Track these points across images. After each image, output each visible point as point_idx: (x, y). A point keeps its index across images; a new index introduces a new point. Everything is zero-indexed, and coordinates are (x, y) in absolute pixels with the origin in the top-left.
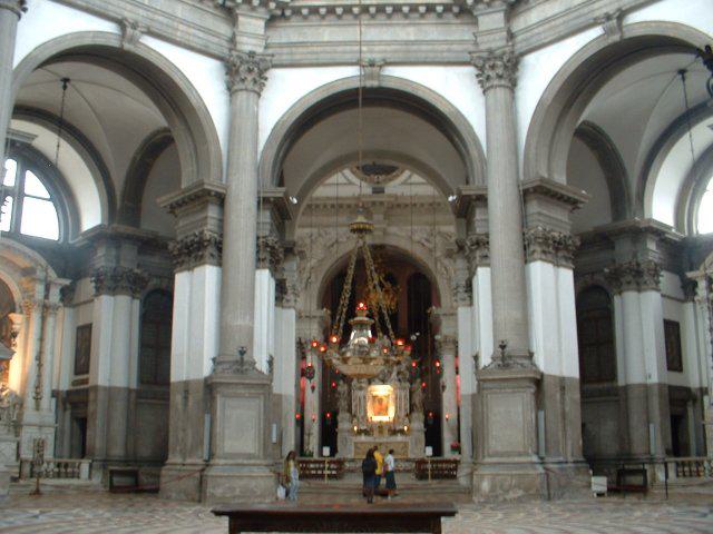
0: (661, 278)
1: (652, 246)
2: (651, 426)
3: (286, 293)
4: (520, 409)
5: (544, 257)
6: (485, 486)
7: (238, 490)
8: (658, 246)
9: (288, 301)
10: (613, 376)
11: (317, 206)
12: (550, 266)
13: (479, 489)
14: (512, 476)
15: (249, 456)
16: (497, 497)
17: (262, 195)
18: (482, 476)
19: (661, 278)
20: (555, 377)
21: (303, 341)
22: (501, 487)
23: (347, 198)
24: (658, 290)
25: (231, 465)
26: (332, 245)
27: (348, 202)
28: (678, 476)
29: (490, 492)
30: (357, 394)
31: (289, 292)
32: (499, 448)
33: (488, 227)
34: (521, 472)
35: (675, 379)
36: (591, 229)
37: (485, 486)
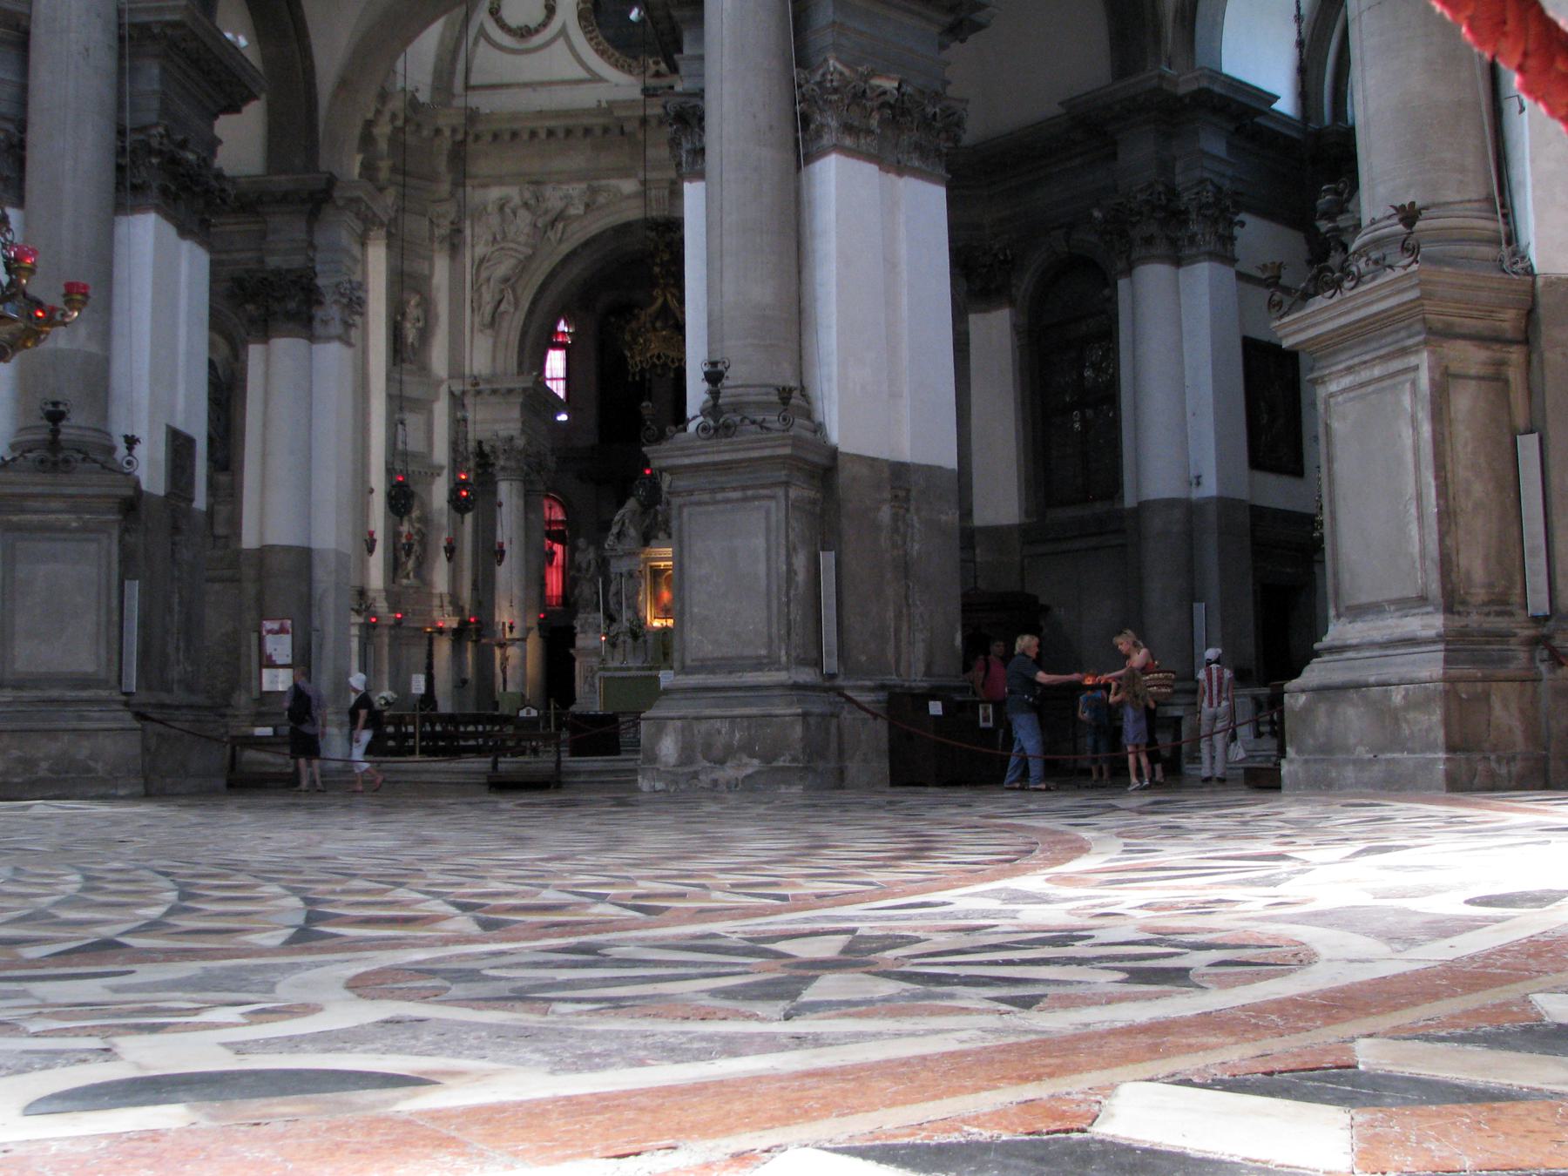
0: (1237, 231)
1: (1215, 145)
2: (1199, 609)
3: (320, 303)
4: (760, 543)
5: (848, 141)
6: (668, 748)
7: (44, 765)
8: (1230, 146)
9: (325, 323)
10: (1114, 487)
11: (514, 135)
12: (871, 169)
13: (652, 758)
14: (733, 717)
15: (84, 682)
16: (695, 775)
17: (126, 19)
18: (661, 723)
19: (1237, 231)
20: (872, 462)
21: (486, 448)
22: (708, 747)
23: (586, 112)
24: (1230, 260)
25: (31, 703)
26: (553, 223)
27: (586, 121)
28: (1259, 735)
29: (681, 764)
30: (618, 566)
31: (329, 299)
32: (709, 650)
33: (702, 76)
34: (754, 711)
35: (1275, 492)
36: (1056, 110)
37: (668, 748)
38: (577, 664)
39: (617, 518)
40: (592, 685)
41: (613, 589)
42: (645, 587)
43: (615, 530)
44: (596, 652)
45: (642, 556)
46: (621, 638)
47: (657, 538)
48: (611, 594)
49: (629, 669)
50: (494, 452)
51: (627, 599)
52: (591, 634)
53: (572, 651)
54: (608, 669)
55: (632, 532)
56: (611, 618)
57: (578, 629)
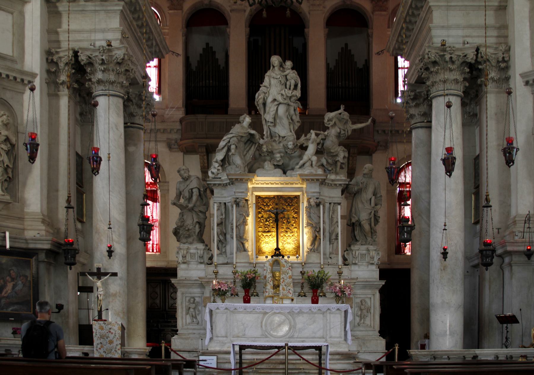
38: (179, 294)
43: (219, 156)
53: (173, 281)
55: (237, 160)
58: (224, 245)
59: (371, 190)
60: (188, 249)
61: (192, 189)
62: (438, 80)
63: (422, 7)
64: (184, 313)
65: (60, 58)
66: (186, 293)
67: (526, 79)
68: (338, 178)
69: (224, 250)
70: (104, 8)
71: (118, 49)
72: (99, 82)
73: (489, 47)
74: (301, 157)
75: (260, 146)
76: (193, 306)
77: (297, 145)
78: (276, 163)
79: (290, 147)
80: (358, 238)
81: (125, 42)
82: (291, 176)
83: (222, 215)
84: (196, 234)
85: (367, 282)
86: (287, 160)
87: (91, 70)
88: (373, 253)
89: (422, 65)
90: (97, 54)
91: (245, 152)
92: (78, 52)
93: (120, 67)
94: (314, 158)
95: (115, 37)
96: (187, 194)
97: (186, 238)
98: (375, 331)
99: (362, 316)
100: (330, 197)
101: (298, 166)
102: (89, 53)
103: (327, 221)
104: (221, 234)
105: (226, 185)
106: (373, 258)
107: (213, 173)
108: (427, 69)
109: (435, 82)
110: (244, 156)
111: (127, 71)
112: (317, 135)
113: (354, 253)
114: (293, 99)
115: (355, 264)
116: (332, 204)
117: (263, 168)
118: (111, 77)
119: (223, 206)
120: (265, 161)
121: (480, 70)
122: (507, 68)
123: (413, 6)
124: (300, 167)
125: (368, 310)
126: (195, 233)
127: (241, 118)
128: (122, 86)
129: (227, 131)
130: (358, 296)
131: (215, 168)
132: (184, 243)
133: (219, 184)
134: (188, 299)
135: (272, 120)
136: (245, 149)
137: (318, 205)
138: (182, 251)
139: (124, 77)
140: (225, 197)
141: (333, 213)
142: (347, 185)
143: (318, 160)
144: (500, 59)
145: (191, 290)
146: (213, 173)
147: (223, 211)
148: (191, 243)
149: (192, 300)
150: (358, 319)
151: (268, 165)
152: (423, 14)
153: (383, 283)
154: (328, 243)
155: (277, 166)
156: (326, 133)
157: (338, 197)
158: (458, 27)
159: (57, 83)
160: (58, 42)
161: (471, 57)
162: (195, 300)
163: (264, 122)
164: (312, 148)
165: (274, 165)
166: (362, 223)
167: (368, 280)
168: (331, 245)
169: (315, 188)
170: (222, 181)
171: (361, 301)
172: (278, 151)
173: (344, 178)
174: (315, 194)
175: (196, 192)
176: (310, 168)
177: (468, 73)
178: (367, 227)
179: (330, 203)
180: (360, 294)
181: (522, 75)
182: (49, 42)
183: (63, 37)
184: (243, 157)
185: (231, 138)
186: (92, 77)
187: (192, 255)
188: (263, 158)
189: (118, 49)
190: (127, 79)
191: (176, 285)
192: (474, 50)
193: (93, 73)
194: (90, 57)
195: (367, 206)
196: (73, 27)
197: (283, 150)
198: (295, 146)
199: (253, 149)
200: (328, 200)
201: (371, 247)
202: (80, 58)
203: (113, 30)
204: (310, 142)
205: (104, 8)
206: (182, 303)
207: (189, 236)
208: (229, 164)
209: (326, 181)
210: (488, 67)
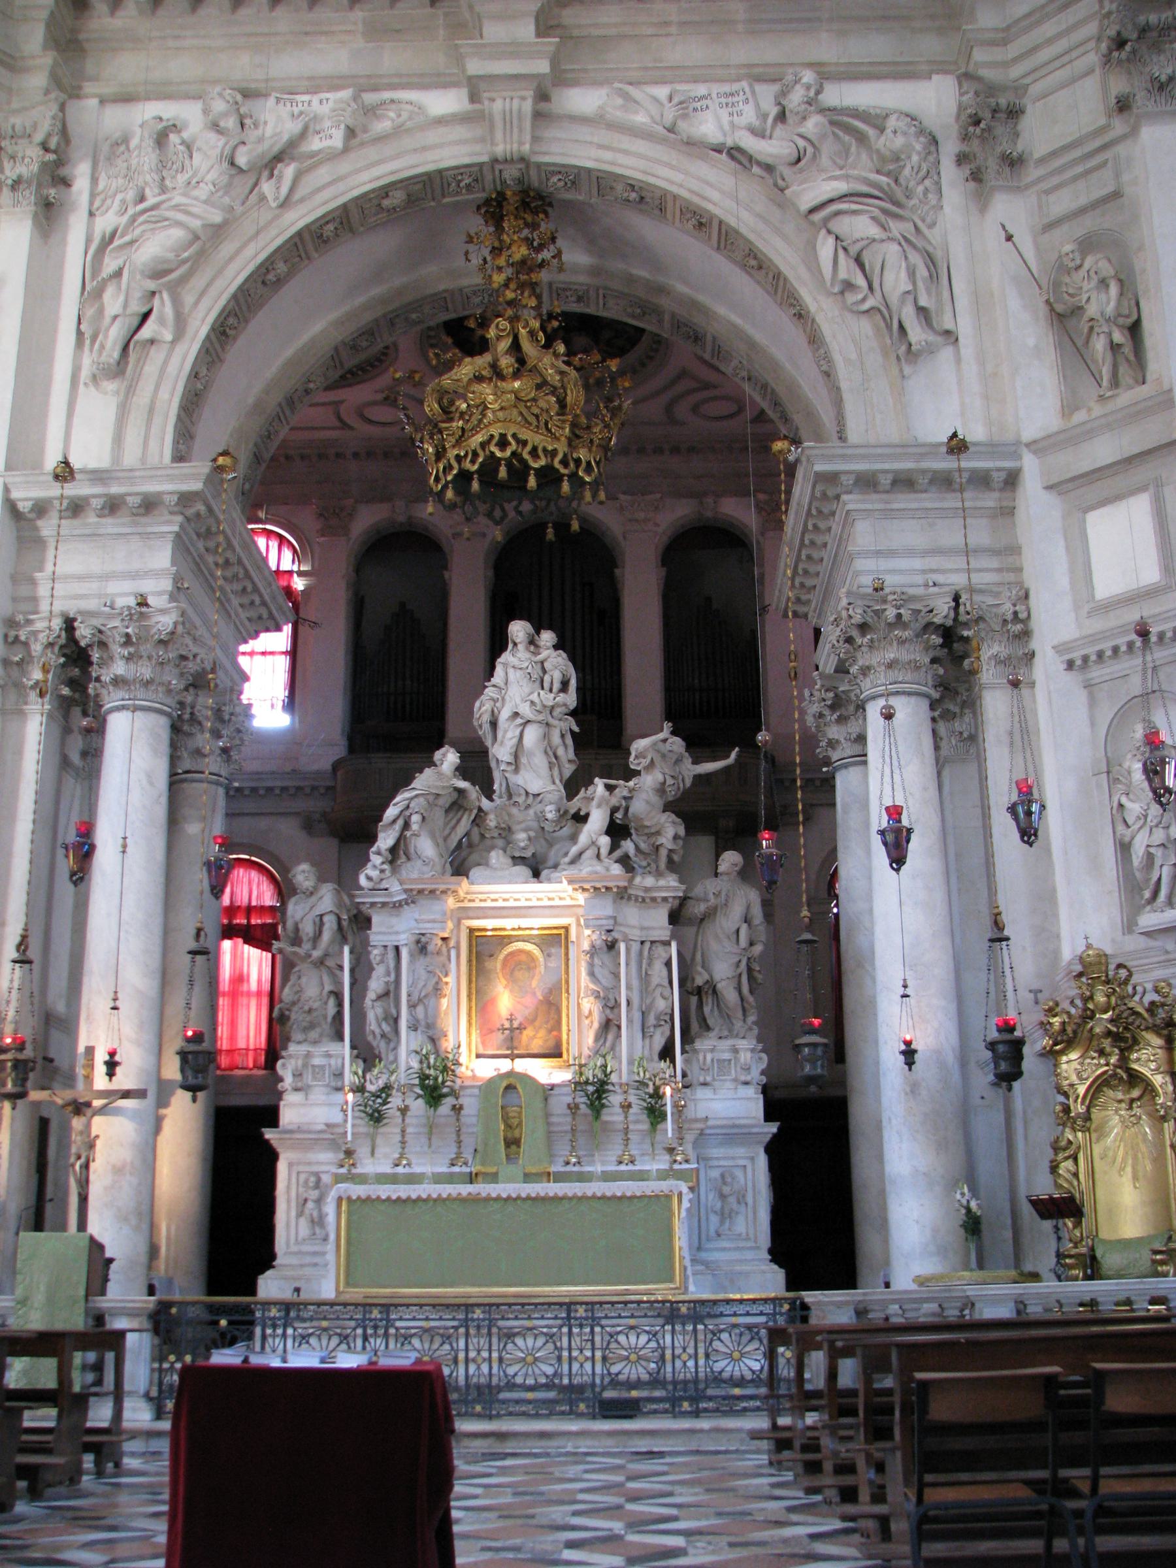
38: (282, 1168)
39: (391, 812)
40: (318, 1222)
41: (375, 985)
42: (455, 980)
43: (385, 840)
44: (331, 1137)
45: (451, 902)
46: (396, 1101)
47: (487, 864)
48: (371, 995)
49: (413, 1179)
50: (103, 645)
51: (412, 1006)
52: (318, 1094)
53: (269, 1134)
54: (362, 1179)
55: (425, 846)
56: (367, 1056)
57: (288, 1081)
58: (392, 1045)
59: (737, 911)
60: (308, 1055)
61: (321, 916)
62: (874, 662)
63: (833, 514)
64: (293, 1213)
65: (35, 633)
66: (299, 1164)
67: (1067, 657)
68: (662, 883)
69: (391, 1058)
70: (140, 530)
71: (163, 611)
72: (117, 681)
73: (981, 592)
74: (574, 838)
75: (480, 817)
76: (314, 1194)
77: (566, 812)
78: (517, 854)
79: (550, 816)
80: (710, 1022)
81: (182, 597)
82: (549, 880)
83: (388, 974)
84: (329, 1019)
85: (734, 1126)
86: (540, 847)
87: (101, 658)
88: (745, 1057)
89: (838, 633)
90: (116, 623)
91: (447, 832)
92: (74, 620)
93: (166, 652)
94: (605, 841)
95: (158, 589)
96: (308, 928)
97: (305, 1030)
98: (758, 1248)
99: (727, 1211)
100: (642, 928)
101: (567, 860)
102: (97, 622)
103: (635, 983)
104: (385, 1019)
105: (401, 906)
106: (748, 1069)
107: (369, 878)
108: (849, 640)
109: (869, 668)
110: (445, 839)
111: (183, 658)
112: (610, 788)
113: (701, 1057)
114: (558, 711)
115: (705, 1084)
116: (647, 945)
117: (487, 864)
118: (144, 670)
119: (391, 954)
120: (493, 848)
121: (967, 640)
122: (1026, 634)
123: (814, 512)
124: (573, 862)
125: (741, 1199)
126: (325, 1017)
127: (438, 755)
128: (169, 691)
129: (405, 781)
130: (716, 1163)
131: (375, 867)
132: (299, 1043)
133: (384, 904)
134: (303, 1177)
135: (510, 759)
136: (446, 824)
137: (611, 946)
138: (293, 1061)
139: (176, 671)
140: (397, 933)
141: (650, 964)
142: (684, 900)
143: (614, 847)
144: (1009, 617)
145: (312, 1156)
146: (369, 878)
147: (392, 964)
148: (315, 1042)
149: (313, 1179)
150: (714, 1219)
151: (497, 857)
152: (836, 528)
153: (773, 1128)
154: (640, 1035)
155: (518, 860)
156: (631, 784)
157: (661, 928)
158: (910, 552)
159: (25, 687)
160: (34, 599)
161: (943, 610)
162: (319, 1180)
163: (493, 764)
164: (598, 819)
165: (513, 858)
166: (719, 986)
167: (737, 1122)
168: (647, 1041)
169: (606, 908)
170: (390, 895)
171: (723, 1176)
172: (523, 826)
173: (676, 884)
174: (604, 922)
175: (330, 923)
176: (595, 862)
177: (942, 646)
178: (730, 995)
179: (642, 943)
180: (718, 1159)
181: (1059, 649)
182: (15, 600)
183: (43, 591)
184: (440, 841)
185: (412, 799)
186: (103, 671)
187: (318, 1071)
188: (488, 842)
189: (163, 611)
190: (182, 674)
191: (274, 1143)
192: (949, 599)
193: (106, 661)
194: (100, 632)
195: (729, 946)
196: (63, 568)
197: (535, 825)
198: (562, 814)
199: (465, 824)
200: (636, 934)
201: (744, 1042)
202: (78, 634)
203: (156, 574)
204: (594, 803)
205: (140, 530)
206: (288, 1187)
207: (312, 1026)
208: (409, 859)
209: (630, 891)
210: (983, 634)
